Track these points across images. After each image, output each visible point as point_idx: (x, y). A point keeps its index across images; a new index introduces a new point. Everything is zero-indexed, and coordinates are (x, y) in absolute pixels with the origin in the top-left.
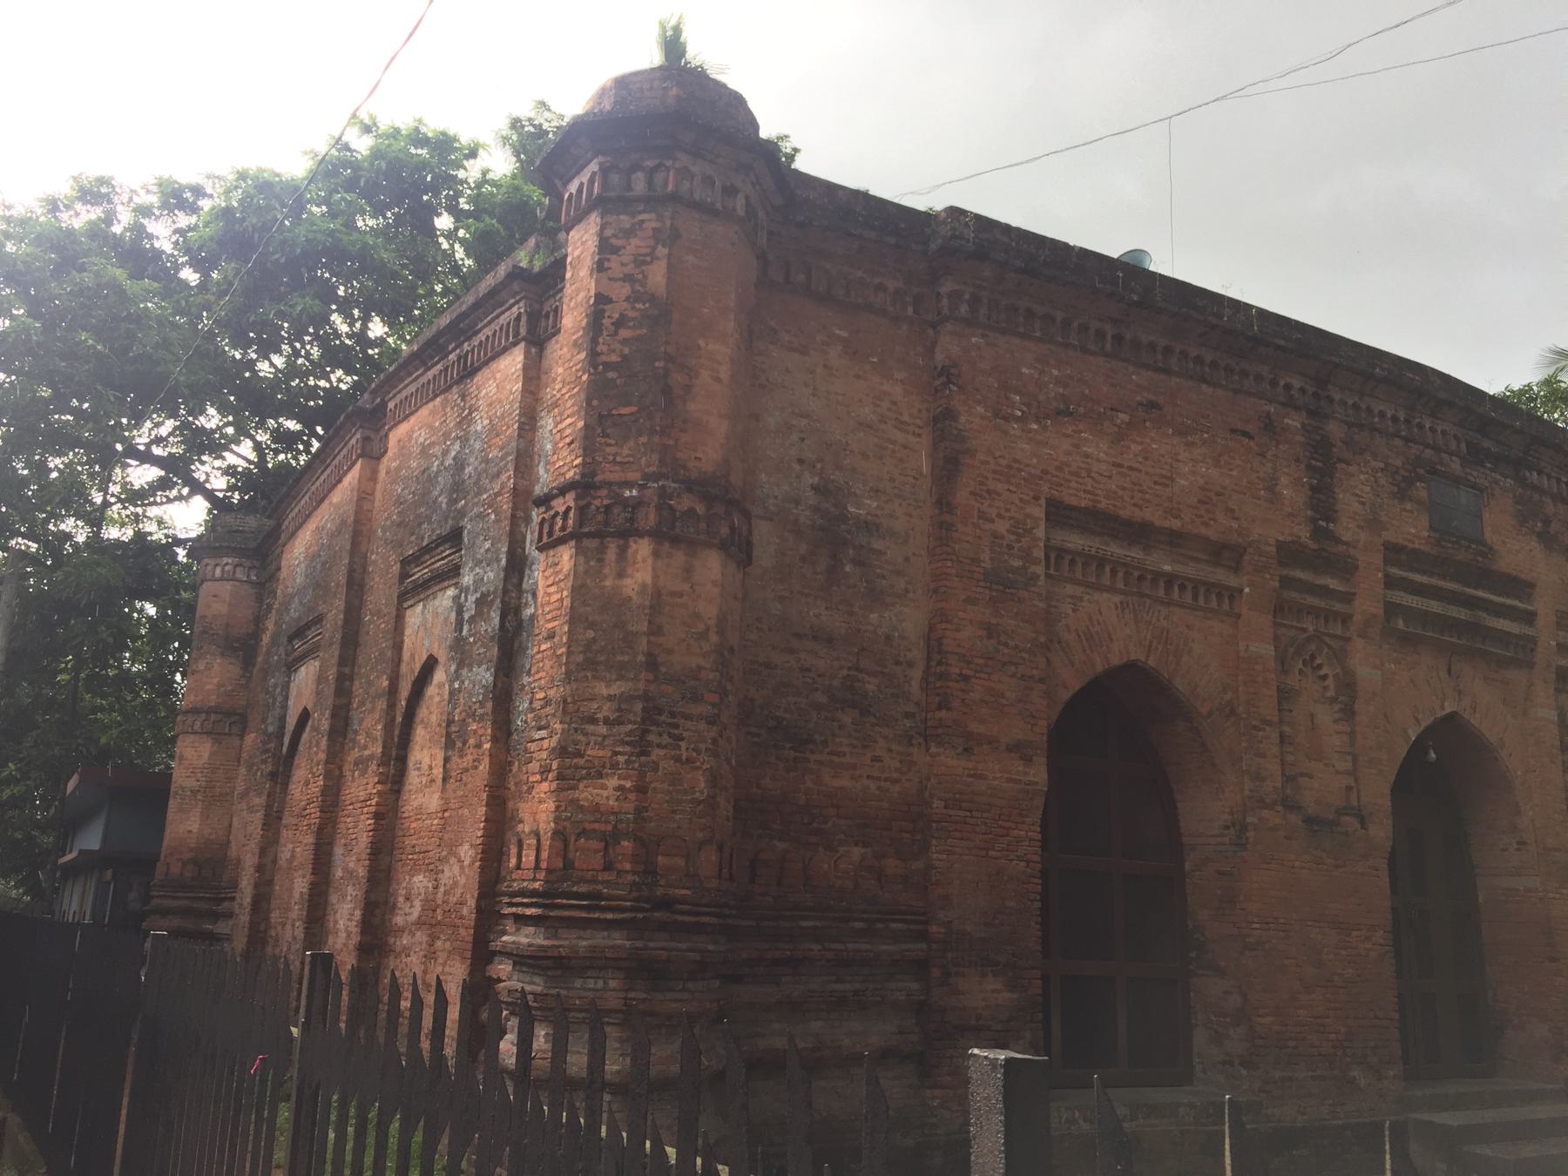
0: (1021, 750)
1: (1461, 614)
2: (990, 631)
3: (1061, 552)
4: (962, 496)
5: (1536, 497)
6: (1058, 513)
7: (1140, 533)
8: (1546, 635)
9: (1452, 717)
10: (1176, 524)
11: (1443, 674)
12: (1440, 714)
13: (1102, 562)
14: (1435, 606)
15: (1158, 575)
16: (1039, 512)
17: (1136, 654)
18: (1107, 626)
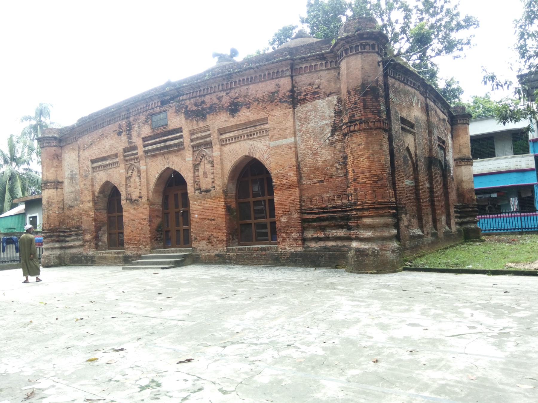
0: (89, 202)
1: (162, 145)
2: (84, 184)
3: (95, 167)
4: (80, 165)
5: (183, 102)
6: (93, 161)
7: (104, 159)
8: (187, 140)
9: (168, 169)
10: (107, 155)
11: (164, 159)
12: (163, 169)
13: (100, 166)
14: (154, 147)
15: (107, 165)
16: (90, 163)
17: (106, 180)
18: (101, 177)
